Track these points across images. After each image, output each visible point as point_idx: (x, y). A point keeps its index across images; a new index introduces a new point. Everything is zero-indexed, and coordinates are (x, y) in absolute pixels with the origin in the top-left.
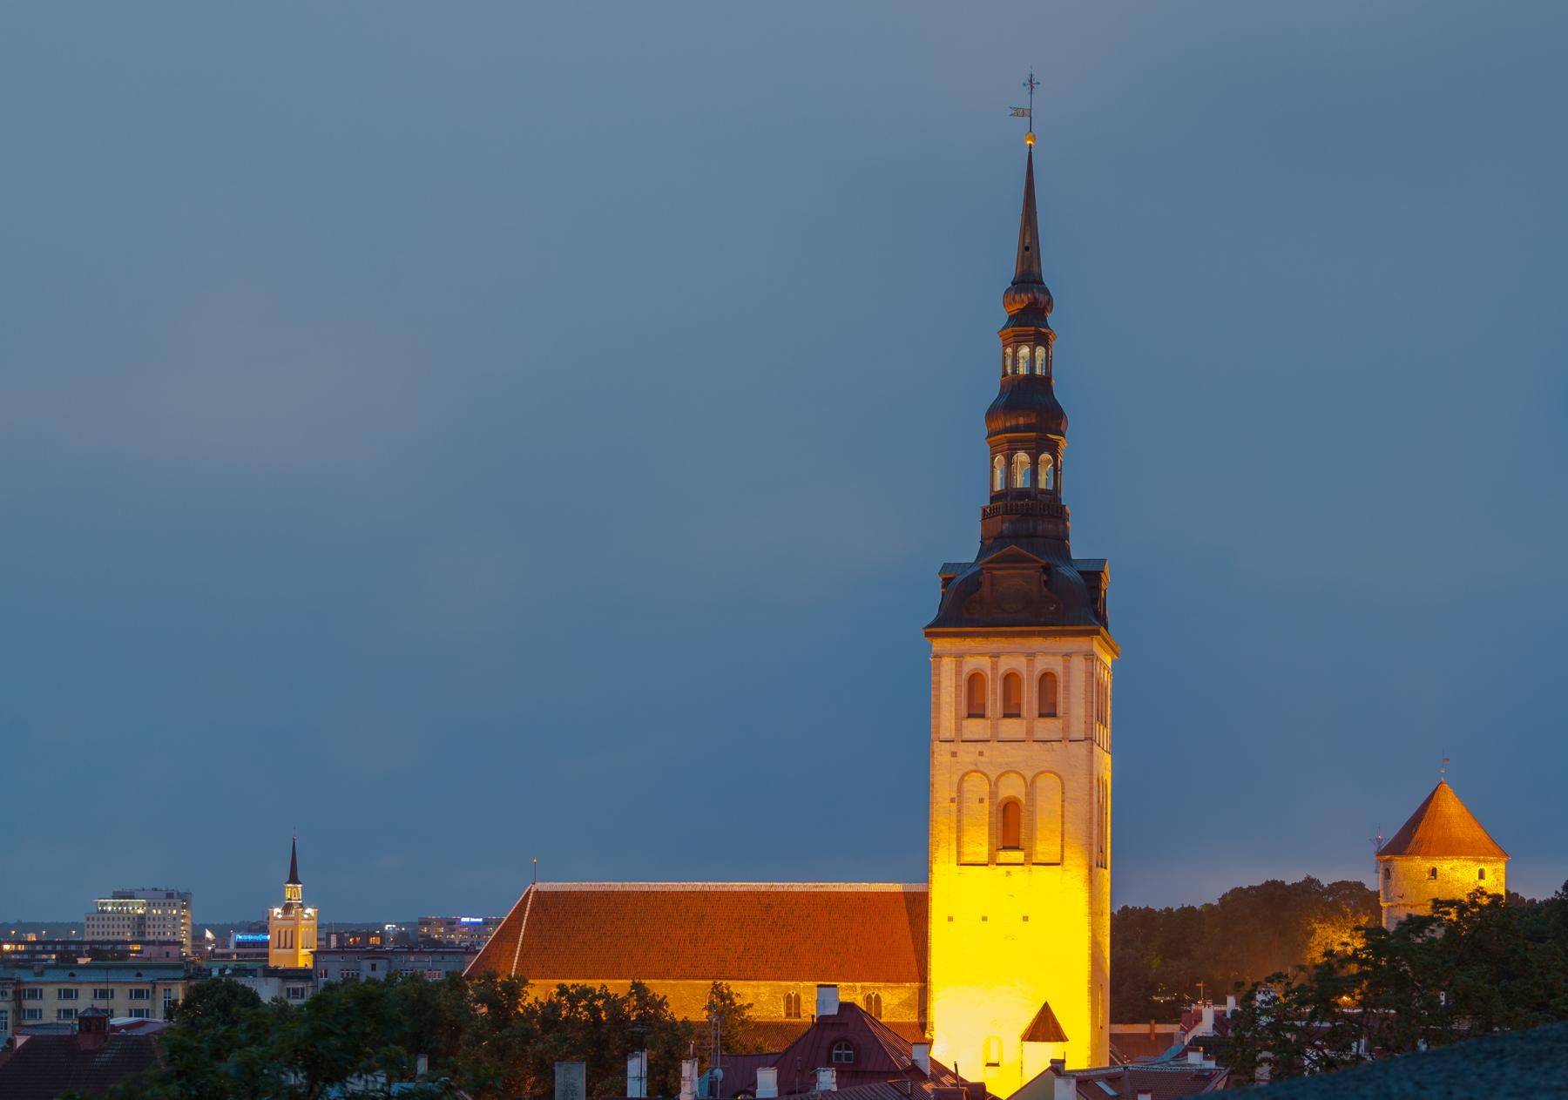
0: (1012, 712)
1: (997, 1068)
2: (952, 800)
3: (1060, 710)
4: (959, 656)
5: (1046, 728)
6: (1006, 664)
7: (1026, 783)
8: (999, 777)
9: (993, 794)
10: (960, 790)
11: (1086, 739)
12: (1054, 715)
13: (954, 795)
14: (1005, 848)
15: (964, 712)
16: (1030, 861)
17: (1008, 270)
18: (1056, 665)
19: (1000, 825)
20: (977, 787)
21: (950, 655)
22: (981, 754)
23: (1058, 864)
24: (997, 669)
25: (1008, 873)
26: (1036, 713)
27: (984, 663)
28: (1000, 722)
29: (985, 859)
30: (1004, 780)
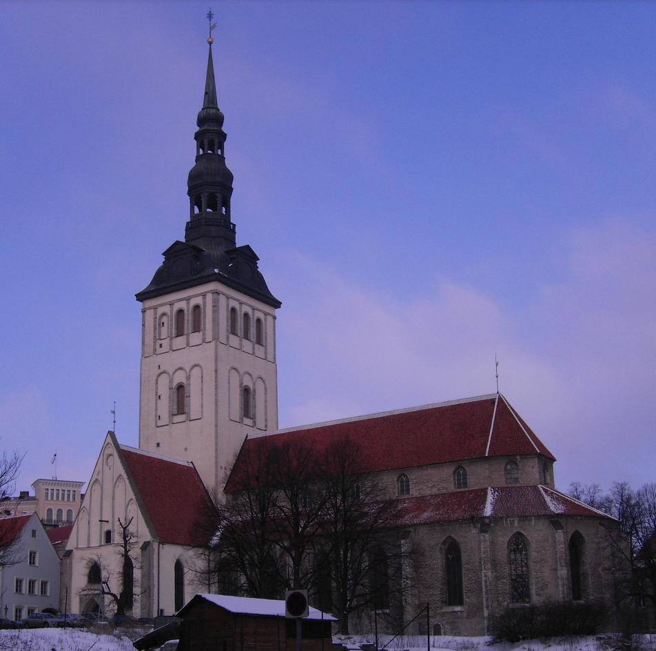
4: (155, 308)
5: (196, 338)
6: (177, 307)
8: (174, 373)
9: (171, 381)
12: (198, 331)
18: (199, 301)
20: (164, 380)
26: (190, 329)
27: (166, 309)
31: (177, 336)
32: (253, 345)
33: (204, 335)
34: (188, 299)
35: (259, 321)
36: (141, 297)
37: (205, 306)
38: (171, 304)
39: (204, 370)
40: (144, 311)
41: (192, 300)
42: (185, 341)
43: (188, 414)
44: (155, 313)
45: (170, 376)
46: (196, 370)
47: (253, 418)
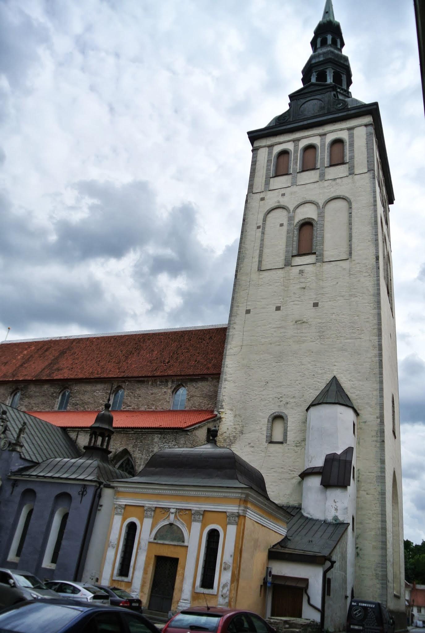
1: (280, 445)
2: (259, 227)
3: (347, 159)
4: (271, 146)
9: (291, 219)
10: (264, 220)
11: (369, 171)
13: (260, 224)
14: (299, 255)
15: (272, 174)
16: (321, 260)
19: (295, 239)
21: (265, 147)
22: (283, 195)
24: (298, 146)
25: (301, 272)
28: (299, 175)
29: (281, 265)
30: (298, 210)
37: (351, 137)
41: (328, 135)
43: (322, 255)
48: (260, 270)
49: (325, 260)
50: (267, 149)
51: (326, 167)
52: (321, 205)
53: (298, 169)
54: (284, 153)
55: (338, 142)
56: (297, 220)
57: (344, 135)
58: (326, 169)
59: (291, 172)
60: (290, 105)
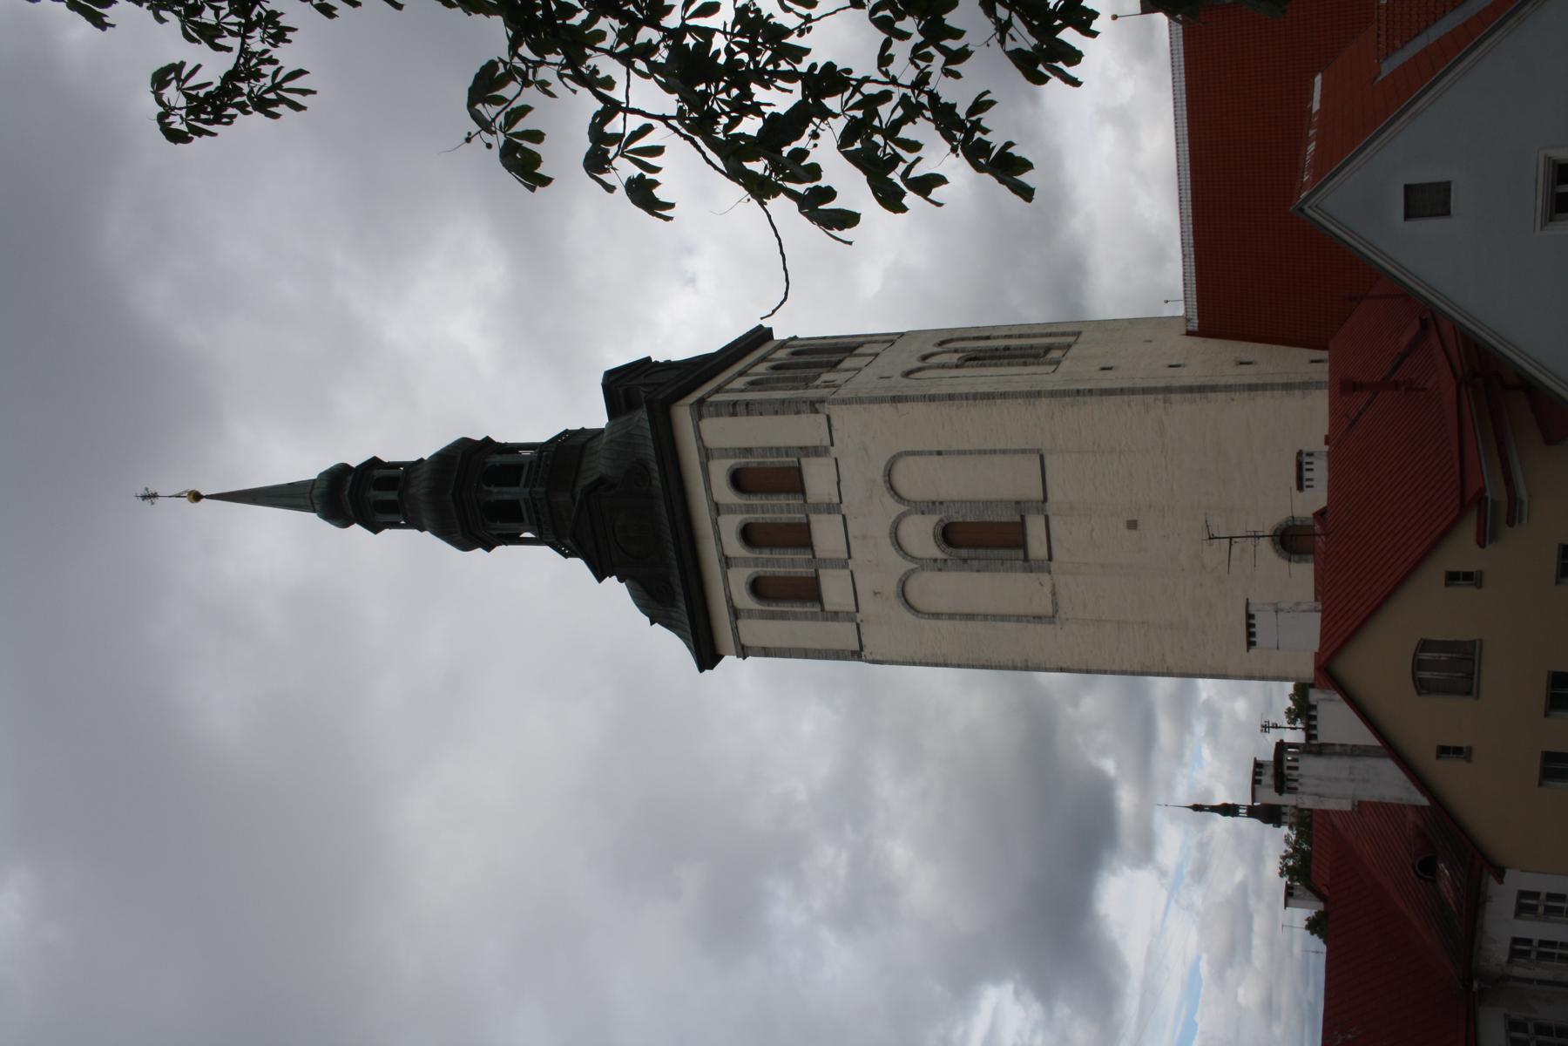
0: (799, 537)
4: (736, 614)
6: (735, 547)
7: (904, 515)
12: (798, 471)
17: (311, 521)
23: (1042, 458)
26: (796, 501)
27: (740, 579)
28: (819, 554)
31: (812, 549)
32: (856, 355)
33: (808, 451)
34: (717, 509)
35: (794, 354)
36: (707, 658)
37: (726, 453)
38: (727, 562)
39: (902, 449)
40: (743, 652)
42: (824, 517)
44: (750, 614)
45: (913, 571)
46: (902, 481)
47: (1048, 349)
48: (1051, 619)
49: (1039, 495)
50: (742, 624)
51: (805, 501)
52: (903, 508)
53: (807, 557)
54: (757, 588)
55: (738, 480)
56: (939, 554)
57: (720, 470)
58: (809, 501)
59: (813, 570)
60: (621, 580)
